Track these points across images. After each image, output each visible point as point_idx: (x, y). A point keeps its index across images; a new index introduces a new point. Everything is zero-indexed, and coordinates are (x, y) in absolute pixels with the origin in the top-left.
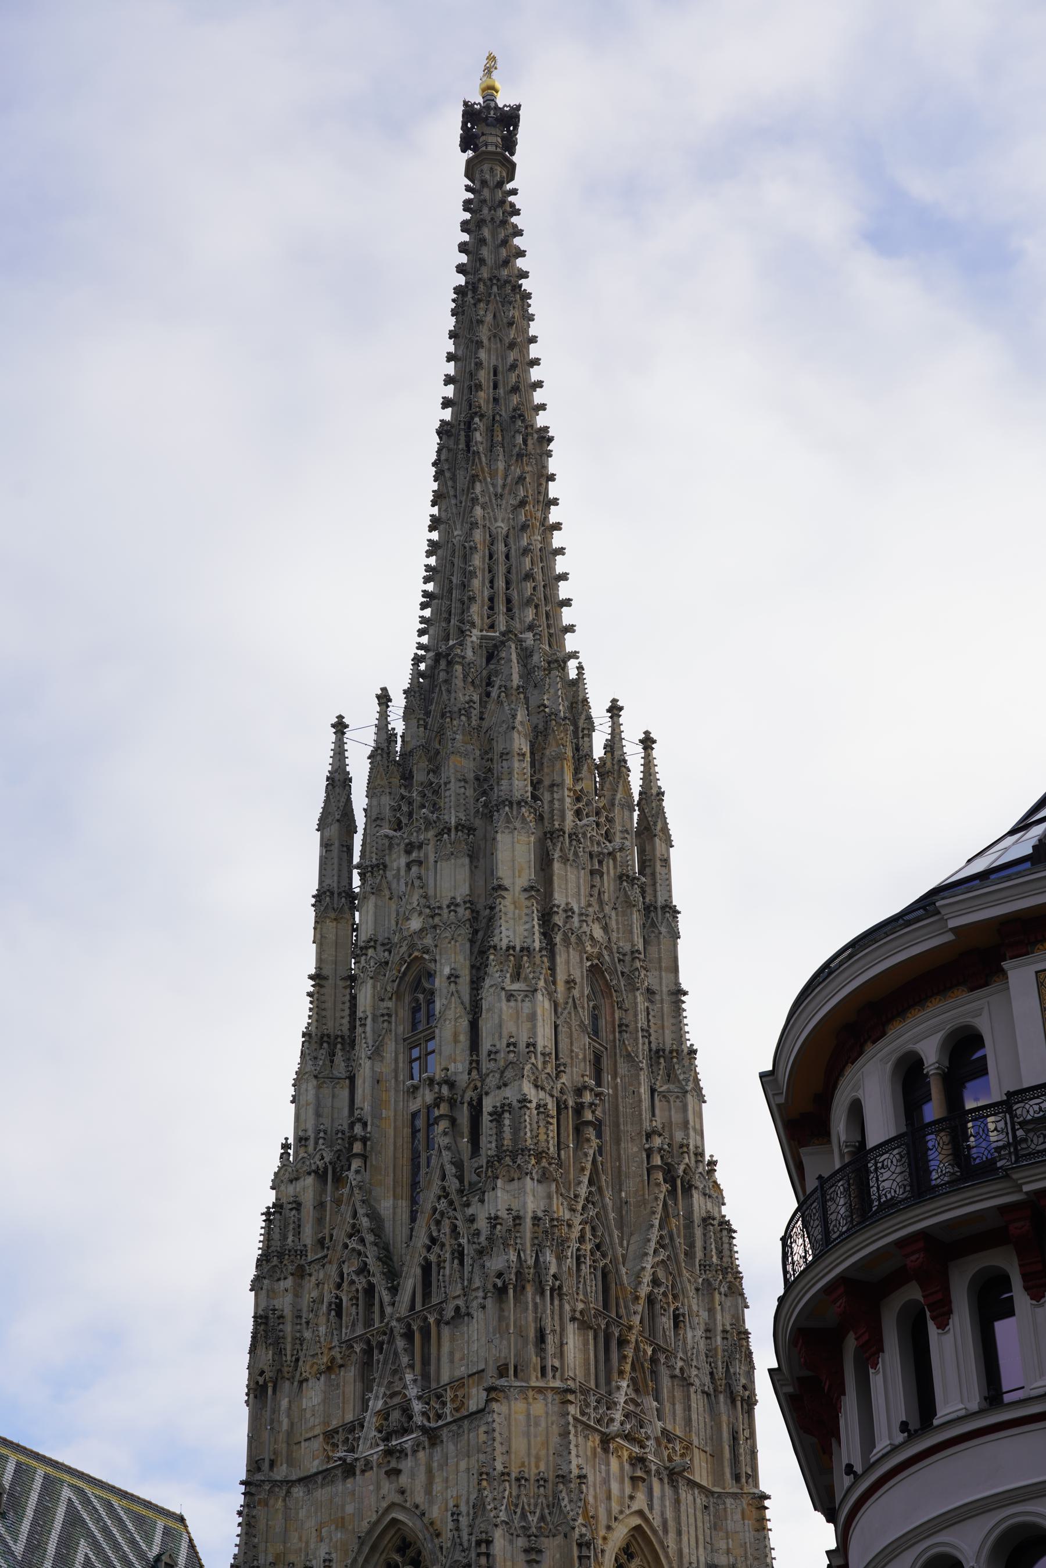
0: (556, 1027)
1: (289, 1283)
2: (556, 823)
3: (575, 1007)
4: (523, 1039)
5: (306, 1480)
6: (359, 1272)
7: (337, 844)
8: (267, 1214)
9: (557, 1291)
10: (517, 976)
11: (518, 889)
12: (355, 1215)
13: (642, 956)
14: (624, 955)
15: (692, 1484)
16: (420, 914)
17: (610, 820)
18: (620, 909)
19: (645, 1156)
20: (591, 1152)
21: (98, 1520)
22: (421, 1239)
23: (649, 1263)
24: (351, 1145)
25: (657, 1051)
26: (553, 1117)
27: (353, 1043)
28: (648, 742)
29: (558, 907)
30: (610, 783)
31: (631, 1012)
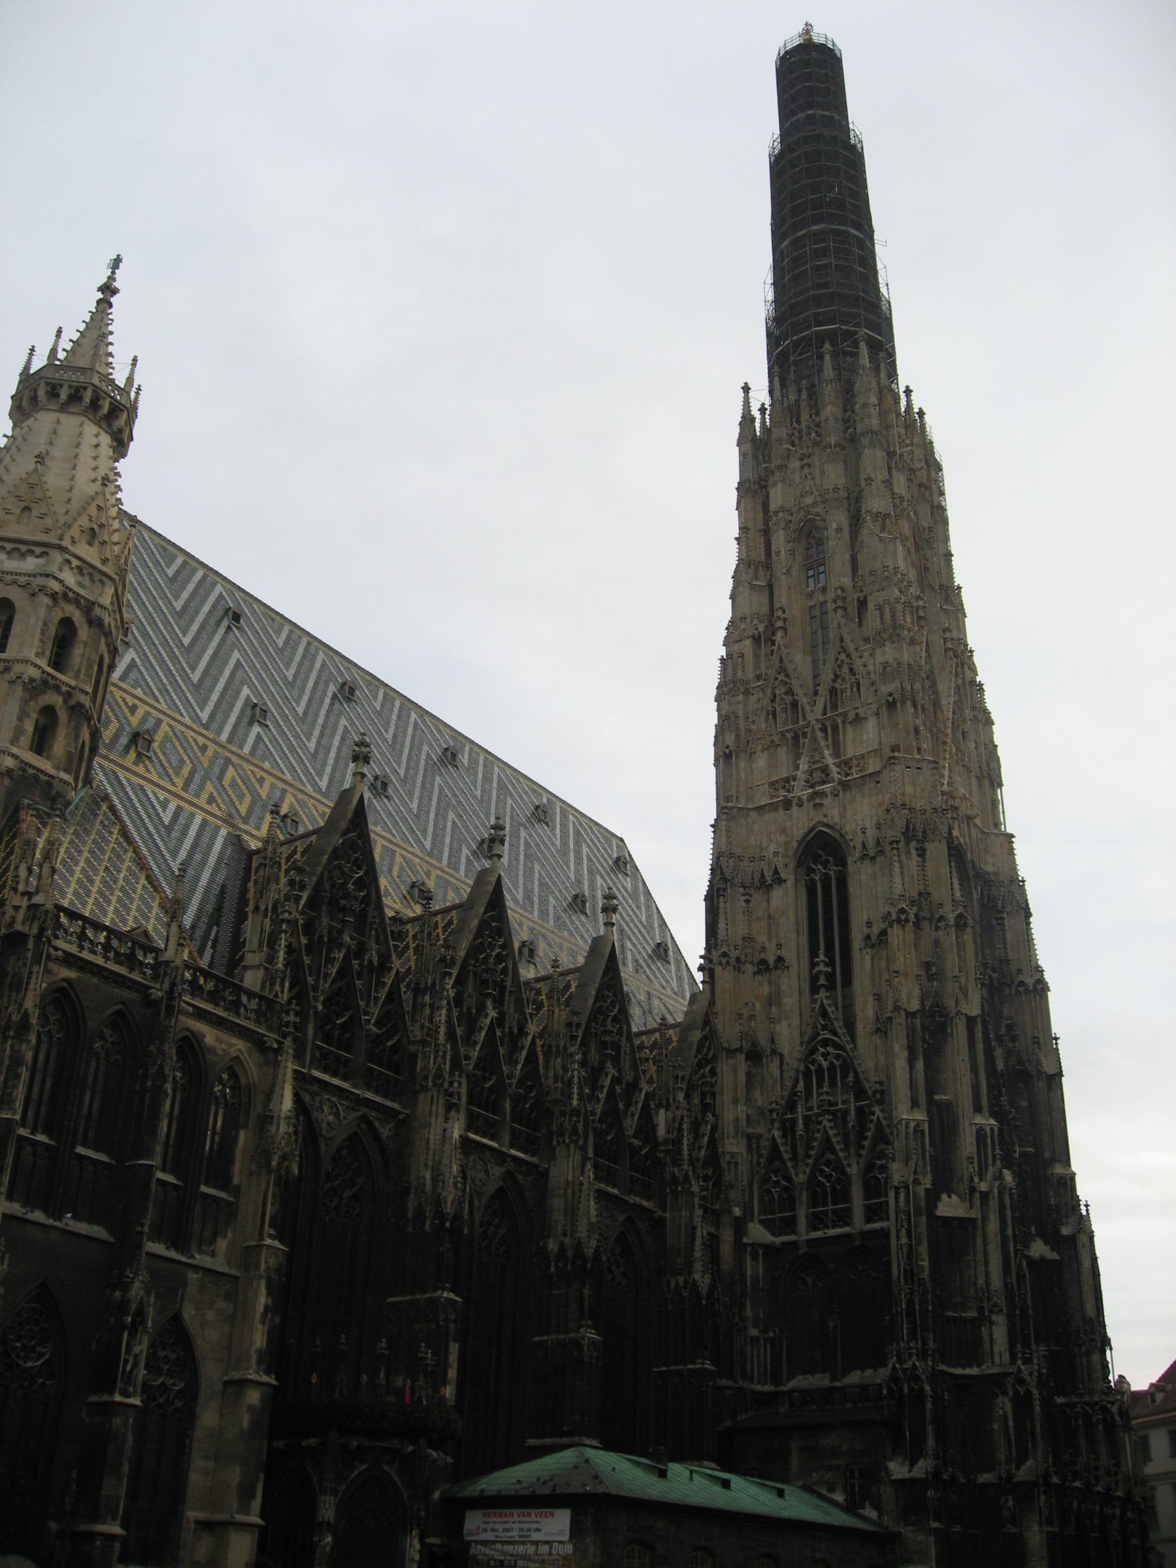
1: (741, 698)
4: (891, 567)
5: (760, 809)
6: (786, 693)
7: (750, 454)
8: (722, 660)
9: (924, 709)
10: (883, 529)
12: (781, 660)
15: (976, 826)
16: (812, 493)
21: (588, 835)
22: (827, 676)
23: (952, 700)
27: (768, 567)
28: (921, 413)
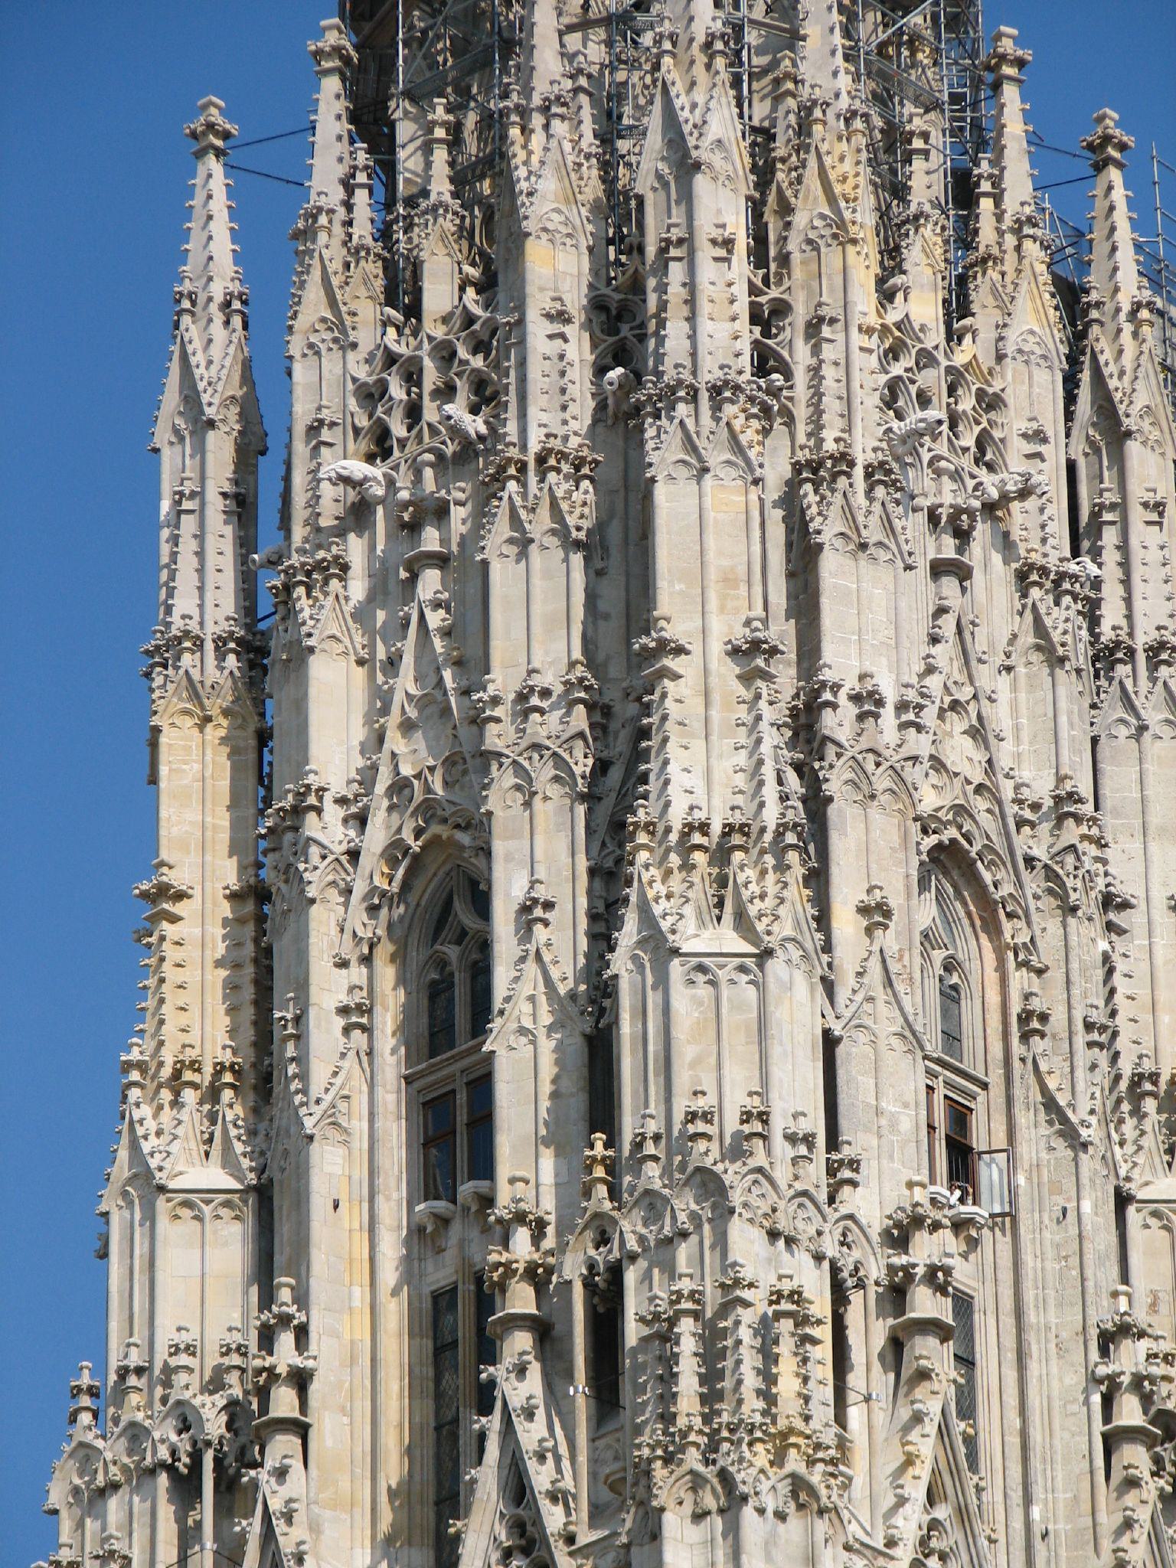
0: (830, 1042)
2: (829, 435)
3: (889, 983)
11: (717, 648)
13: (1088, 809)
14: (1035, 807)
17: (991, 402)
18: (1021, 670)
19: (1096, 1399)
20: (934, 1407)
24: (263, 1394)
25: (1137, 1080)
26: (819, 1322)
29: (836, 688)
30: (994, 291)
31: (1056, 975)
